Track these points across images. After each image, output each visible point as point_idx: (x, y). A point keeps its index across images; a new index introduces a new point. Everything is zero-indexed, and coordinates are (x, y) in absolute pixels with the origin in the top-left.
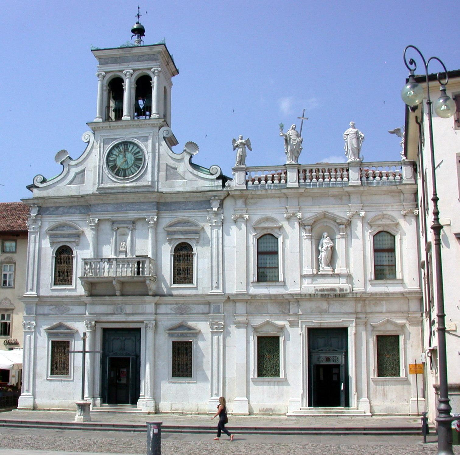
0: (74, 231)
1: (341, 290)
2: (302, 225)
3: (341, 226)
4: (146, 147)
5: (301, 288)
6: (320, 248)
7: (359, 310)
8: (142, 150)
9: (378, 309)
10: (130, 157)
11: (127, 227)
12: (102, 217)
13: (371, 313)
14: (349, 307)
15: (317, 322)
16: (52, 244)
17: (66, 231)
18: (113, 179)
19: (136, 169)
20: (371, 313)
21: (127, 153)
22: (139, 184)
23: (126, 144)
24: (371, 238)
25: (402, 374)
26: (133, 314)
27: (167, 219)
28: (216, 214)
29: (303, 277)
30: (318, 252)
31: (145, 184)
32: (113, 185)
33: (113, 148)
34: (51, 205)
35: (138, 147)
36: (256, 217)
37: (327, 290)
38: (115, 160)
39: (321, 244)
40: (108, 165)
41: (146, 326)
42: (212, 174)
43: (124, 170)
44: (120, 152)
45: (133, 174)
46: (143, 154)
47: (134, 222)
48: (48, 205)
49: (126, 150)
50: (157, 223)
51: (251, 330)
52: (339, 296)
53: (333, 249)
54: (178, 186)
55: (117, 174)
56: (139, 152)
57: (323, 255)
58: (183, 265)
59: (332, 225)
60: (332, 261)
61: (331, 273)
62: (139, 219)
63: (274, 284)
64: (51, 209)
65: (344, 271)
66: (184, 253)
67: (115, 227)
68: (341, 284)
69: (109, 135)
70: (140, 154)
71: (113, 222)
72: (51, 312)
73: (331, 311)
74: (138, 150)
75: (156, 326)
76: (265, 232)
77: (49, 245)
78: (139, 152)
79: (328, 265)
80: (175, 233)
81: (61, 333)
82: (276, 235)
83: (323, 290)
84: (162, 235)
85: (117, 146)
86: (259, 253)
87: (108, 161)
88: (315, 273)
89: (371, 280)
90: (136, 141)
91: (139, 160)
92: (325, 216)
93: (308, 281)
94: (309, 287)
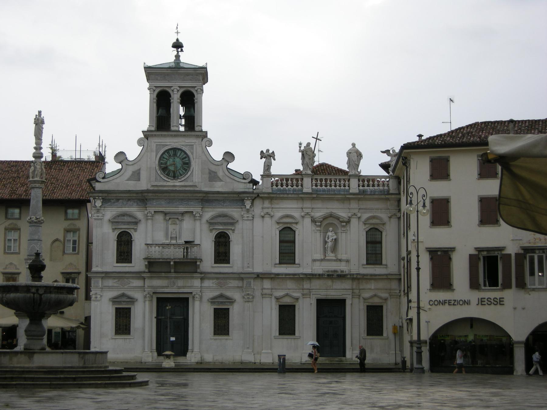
0: (134, 220)
1: (342, 271)
2: (314, 221)
3: (343, 224)
4: (192, 153)
5: (312, 269)
6: (327, 239)
7: (354, 287)
8: (188, 156)
9: (368, 286)
10: (178, 160)
11: (178, 219)
12: (157, 209)
13: (363, 289)
14: (347, 285)
15: (324, 294)
16: (114, 230)
17: (127, 219)
18: (165, 179)
19: (184, 171)
20: (363, 289)
21: (176, 158)
22: (187, 184)
23: (175, 150)
24: (365, 234)
25: (385, 334)
26: (184, 287)
27: (209, 213)
28: (248, 211)
29: (314, 261)
30: (325, 242)
31: (191, 184)
32: (165, 184)
33: (164, 153)
34: (113, 198)
35: (185, 153)
36: (278, 214)
37: (332, 271)
38: (166, 163)
39: (327, 237)
40: (160, 167)
41: (193, 297)
42: (244, 179)
43: (174, 172)
44: (170, 156)
45: (181, 175)
46: (189, 160)
47: (183, 214)
48: (110, 198)
49: (175, 155)
50: (201, 216)
51: (274, 300)
52: (342, 276)
53: (336, 241)
54: (218, 187)
55: (168, 175)
56: (185, 158)
57: (330, 244)
58: (222, 249)
59: (336, 222)
60: (334, 249)
61: (334, 258)
62: (187, 212)
63: (292, 266)
64: (112, 201)
65: (344, 257)
66: (222, 240)
67: (168, 218)
68: (342, 267)
69: (161, 142)
70: (187, 159)
71: (166, 214)
72: (115, 285)
73: (335, 287)
74: (185, 156)
75: (201, 297)
76: (286, 226)
77: (111, 231)
78: (185, 158)
79: (332, 252)
80: (216, 224)
81: (124, 302)
82: (294, 229)
83: (328, 271)
84: (205, 227)
85: (167, 151)
86: (281, 242)
87: (160, 164)
88: (323, 258)
89: (363, 265)
90: (184, 148)
91: (187, 165)
92: (331, 216)
93: (318, 263)
94: (319, 268)
